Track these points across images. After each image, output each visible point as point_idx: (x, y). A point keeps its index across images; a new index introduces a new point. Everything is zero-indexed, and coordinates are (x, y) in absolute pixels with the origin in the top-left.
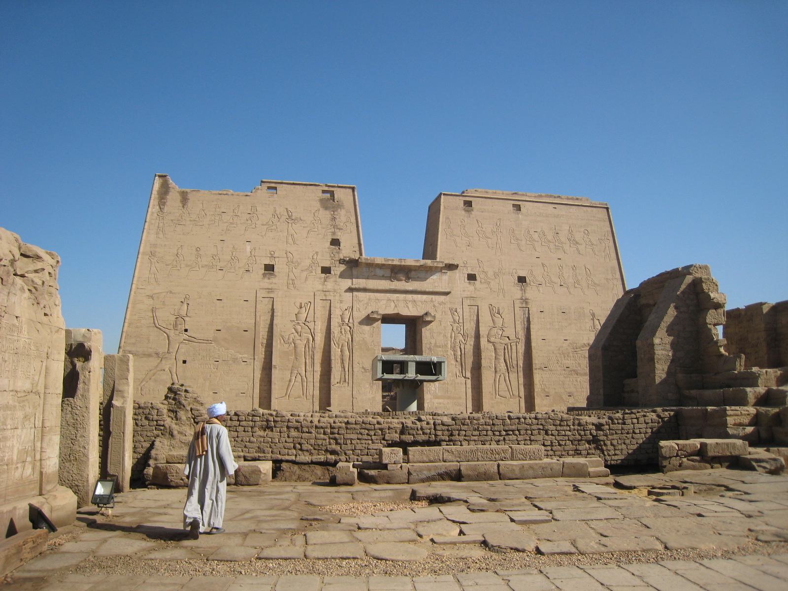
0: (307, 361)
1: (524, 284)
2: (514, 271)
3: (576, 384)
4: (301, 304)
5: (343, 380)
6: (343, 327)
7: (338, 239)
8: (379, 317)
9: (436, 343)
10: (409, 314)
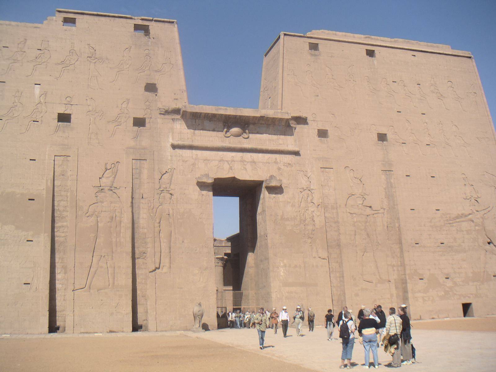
1: (384, 142)
4: (106, 164)
6: (162, 194)
7: (156, 84)
8: (210, 181)
10: (247, 178)
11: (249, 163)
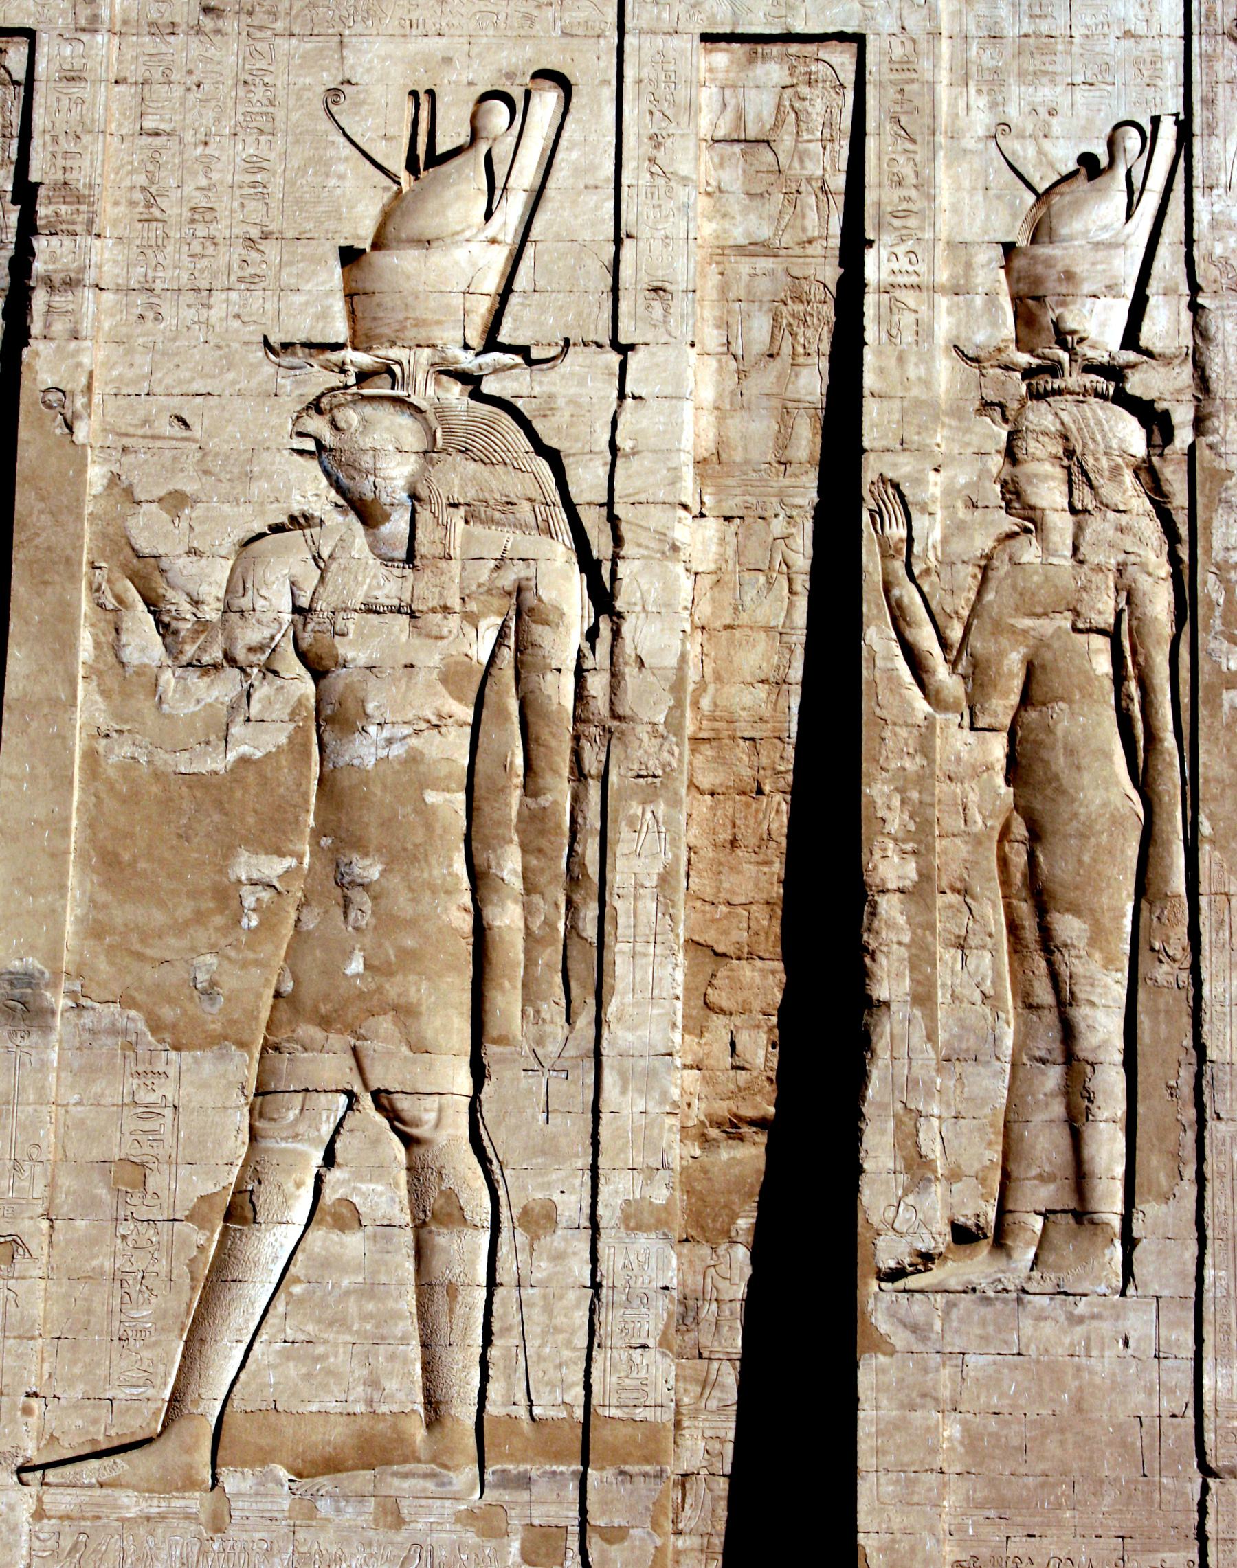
0: (507, 918)
4: (424, 99)
5: (1038, 1195)
6: (1041, 417)
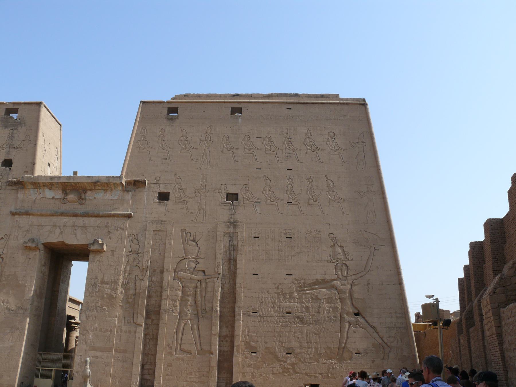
2: (223, 186)
3: (300, 336)
8: (34, 246)
9: (103, 279)
11: (80, 228)
